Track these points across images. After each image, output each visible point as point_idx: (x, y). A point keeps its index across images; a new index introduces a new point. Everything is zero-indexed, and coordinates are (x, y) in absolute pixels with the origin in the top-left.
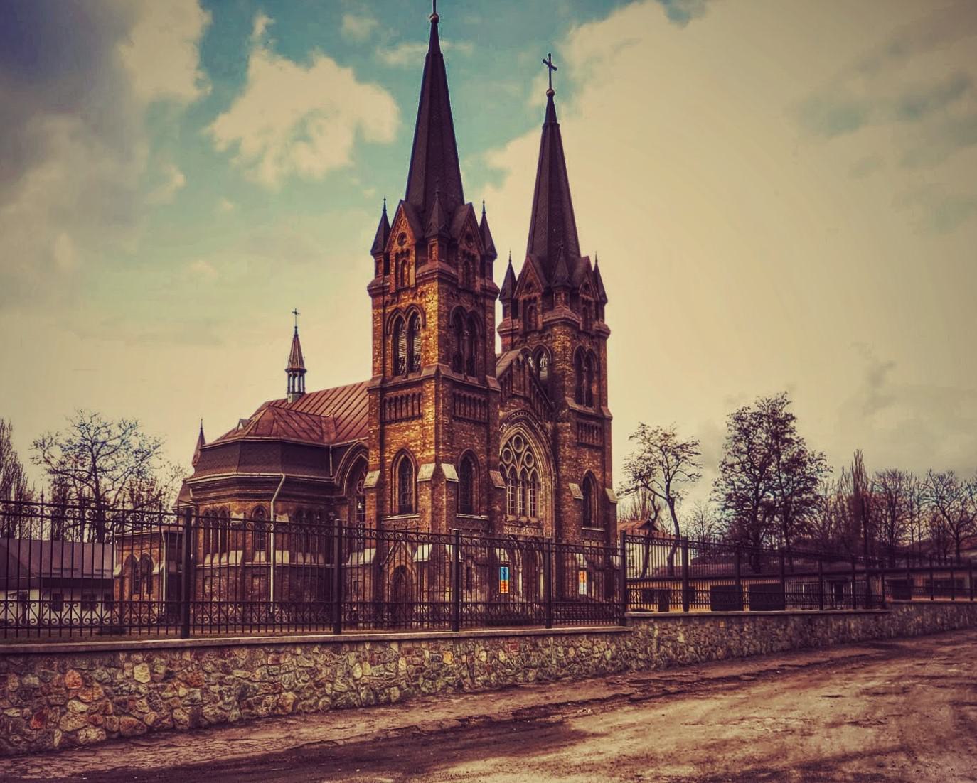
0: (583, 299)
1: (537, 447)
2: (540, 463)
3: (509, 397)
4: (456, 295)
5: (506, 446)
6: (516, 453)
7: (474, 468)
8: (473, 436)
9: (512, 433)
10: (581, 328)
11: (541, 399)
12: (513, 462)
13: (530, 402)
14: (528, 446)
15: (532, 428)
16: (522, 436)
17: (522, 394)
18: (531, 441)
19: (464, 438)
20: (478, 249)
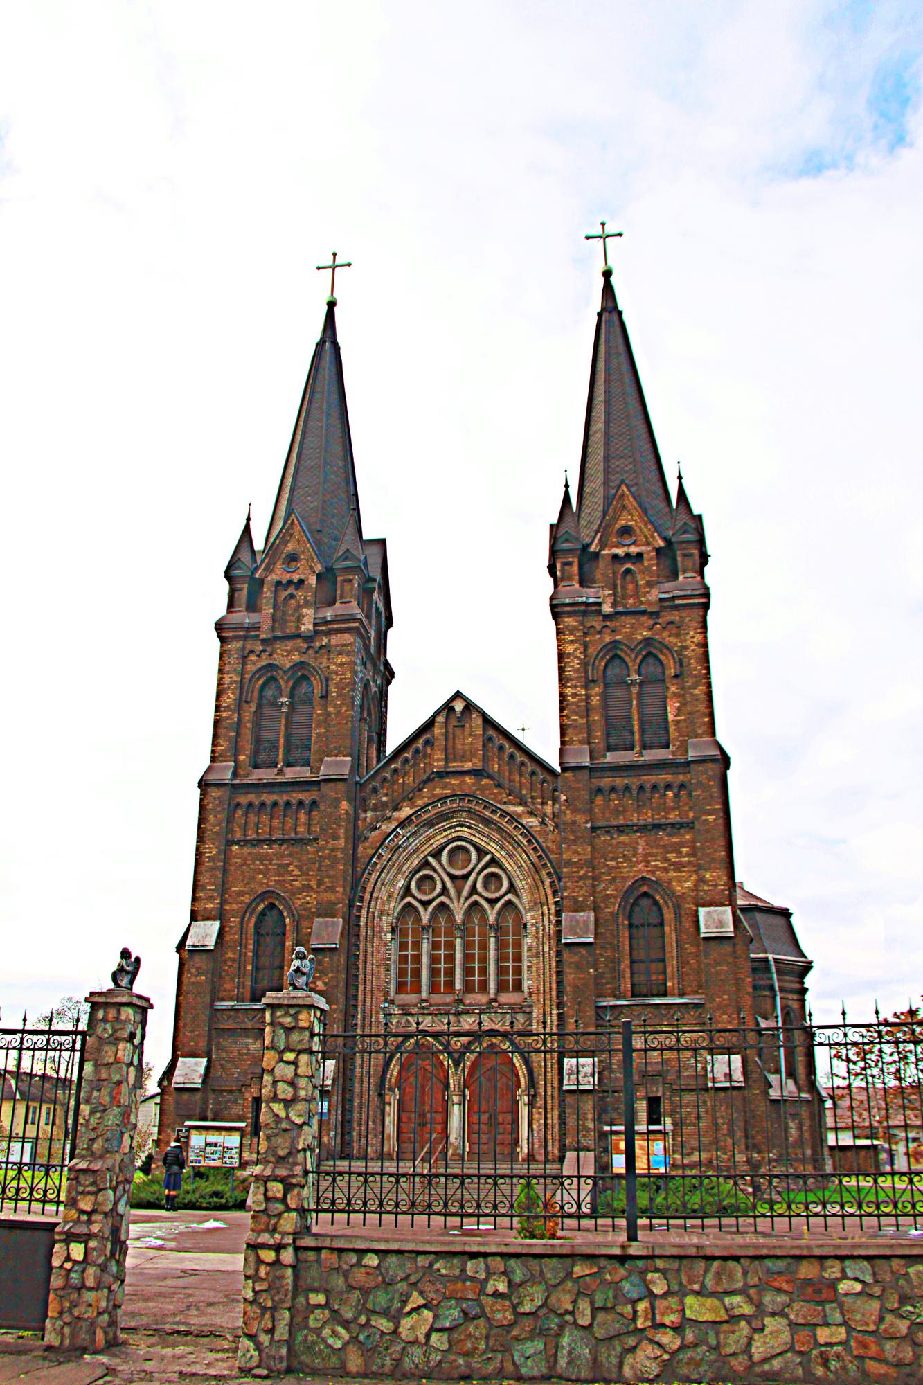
0: (615, 557)
1: (511, 856)
2: (519, 884)
3: (429, 780)
4: (263, 651)
5: (425, 864)
6: (452, 877)
7: (287, 920)
8: (288, 865)
9: (440, 840)
10: (607, 609)
11: (523, 764)
12: (444, 891)
13: (489, 777)
14: (488, 857)
15: (487, 822)
16: (470, 842)
17: (468, 766)
18: (492, 847)
19: (261, 872)
20: (311, 567)
